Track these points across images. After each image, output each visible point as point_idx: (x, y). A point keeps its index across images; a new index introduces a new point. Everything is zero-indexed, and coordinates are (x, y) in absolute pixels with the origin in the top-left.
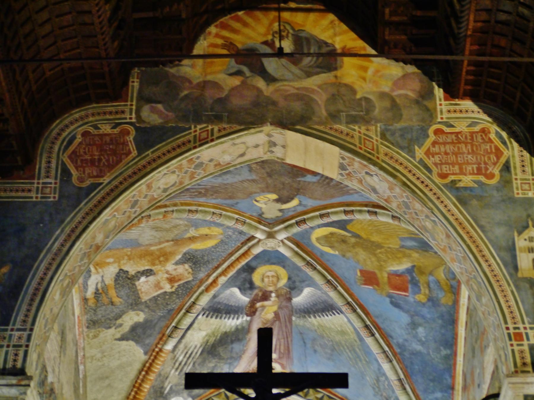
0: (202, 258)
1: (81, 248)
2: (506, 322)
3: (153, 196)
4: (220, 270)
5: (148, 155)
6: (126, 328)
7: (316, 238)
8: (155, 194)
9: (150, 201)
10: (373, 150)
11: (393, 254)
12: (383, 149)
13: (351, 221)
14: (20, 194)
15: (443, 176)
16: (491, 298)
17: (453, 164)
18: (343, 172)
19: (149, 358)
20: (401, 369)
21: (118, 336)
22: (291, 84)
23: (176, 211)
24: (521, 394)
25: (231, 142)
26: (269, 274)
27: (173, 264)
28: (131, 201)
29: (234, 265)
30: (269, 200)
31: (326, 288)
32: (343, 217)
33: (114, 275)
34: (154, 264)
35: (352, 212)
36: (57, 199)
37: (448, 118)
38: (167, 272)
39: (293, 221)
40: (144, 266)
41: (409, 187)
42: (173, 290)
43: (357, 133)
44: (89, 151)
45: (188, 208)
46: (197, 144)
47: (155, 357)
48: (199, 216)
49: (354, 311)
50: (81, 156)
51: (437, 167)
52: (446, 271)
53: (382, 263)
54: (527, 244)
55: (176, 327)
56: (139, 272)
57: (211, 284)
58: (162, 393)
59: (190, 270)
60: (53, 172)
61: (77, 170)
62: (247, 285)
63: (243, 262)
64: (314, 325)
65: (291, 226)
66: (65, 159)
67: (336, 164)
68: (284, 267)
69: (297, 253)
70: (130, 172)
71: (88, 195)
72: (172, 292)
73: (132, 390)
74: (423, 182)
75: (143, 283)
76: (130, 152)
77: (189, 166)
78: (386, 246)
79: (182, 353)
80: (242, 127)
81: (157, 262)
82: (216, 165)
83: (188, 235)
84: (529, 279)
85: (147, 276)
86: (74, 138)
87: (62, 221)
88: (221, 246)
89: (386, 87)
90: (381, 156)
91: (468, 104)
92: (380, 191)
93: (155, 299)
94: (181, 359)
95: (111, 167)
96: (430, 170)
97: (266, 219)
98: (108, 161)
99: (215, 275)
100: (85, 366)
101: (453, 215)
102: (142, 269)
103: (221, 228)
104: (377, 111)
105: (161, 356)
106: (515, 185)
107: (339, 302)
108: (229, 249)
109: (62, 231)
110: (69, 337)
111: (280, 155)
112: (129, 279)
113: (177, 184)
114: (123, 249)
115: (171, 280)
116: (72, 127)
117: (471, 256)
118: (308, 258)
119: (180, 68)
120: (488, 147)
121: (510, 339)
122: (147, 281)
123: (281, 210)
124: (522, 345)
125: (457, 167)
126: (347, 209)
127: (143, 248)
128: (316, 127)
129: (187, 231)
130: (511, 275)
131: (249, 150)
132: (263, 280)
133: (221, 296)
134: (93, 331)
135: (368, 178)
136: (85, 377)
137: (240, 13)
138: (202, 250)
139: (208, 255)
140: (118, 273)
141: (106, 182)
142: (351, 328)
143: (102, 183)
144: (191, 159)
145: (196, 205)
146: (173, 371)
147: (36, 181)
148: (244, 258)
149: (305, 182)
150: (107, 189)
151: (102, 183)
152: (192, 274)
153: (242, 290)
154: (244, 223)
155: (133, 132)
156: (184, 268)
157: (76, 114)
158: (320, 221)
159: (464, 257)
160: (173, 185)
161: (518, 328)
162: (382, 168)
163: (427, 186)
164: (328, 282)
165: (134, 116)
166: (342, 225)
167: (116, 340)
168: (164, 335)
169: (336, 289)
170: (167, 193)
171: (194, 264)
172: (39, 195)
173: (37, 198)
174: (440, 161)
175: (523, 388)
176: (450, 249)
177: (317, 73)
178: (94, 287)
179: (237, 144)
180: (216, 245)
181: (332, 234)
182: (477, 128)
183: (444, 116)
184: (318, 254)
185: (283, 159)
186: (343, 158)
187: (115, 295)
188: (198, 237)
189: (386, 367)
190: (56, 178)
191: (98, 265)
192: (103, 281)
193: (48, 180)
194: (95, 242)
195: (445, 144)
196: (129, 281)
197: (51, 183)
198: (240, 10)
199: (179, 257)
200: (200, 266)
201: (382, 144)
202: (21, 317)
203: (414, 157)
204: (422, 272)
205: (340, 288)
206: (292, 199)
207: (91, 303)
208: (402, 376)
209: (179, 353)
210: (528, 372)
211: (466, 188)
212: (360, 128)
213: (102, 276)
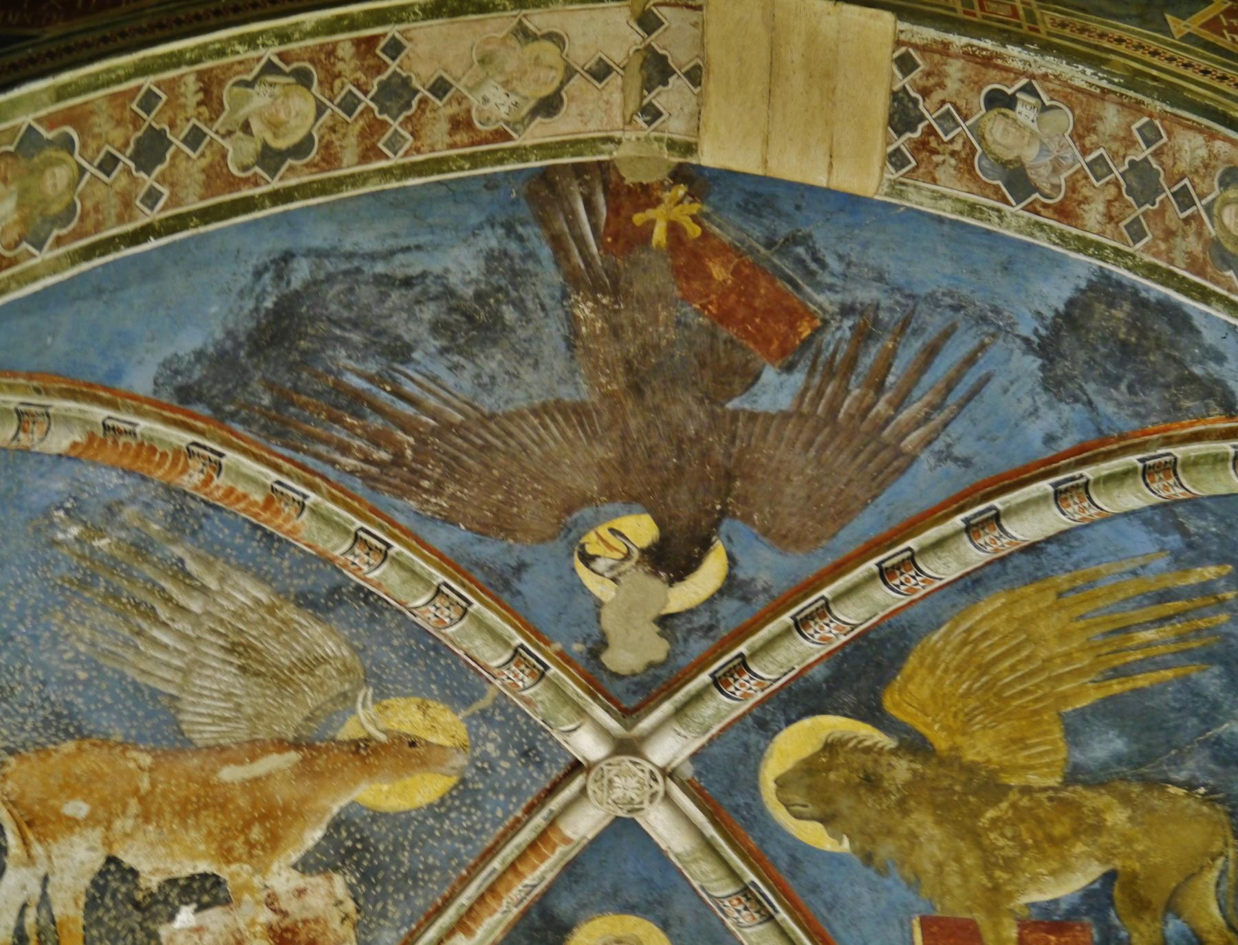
0: (393, 854)
7: (776, 781)
11: (1040, 822)
18: (902, 142)
27: (295, 867)
29: (501, 889)
30: (627, 556)
33: (86, 882)
34: (226, 856)
35: (911, 560)
38: (271, 901)
39: (704, 678)
40: (194, 857)
52: (1223, 888)
53: (1000, 875)
56: (173, 882)
59: (350, 906)
65: (698, 697)
67: (880, 107)
69: (709, 846)
77: (363, 78)
78: (1014, 781)
81: (239, 846)
83: (348, 731)
85: (202, 907)
88: (458, 809)
102: (185, 868)
103: (464, 713)
108: (483, 830)
111: (676, 127)
112: (137, 905)
113: (313, 155)
114: (124, 746)
118: (750, 876)
122: (199, 930)
123: (665, 622)
126: (891, 556)
131: (576, 80)
139: (413, 845)
140: (102, 874)
144: (372, 41)
148: (533, 858)
149: (753, 417)
152: (356, 925)
156: (331, 894)
171: (365, 878)
179: (535, 38)
180: (442, 801)
181: (831, 747)
184: (783, 861)
185: (690, 148)
186: (905, 64)
188: (382, 745)
192: (44, 900)
196: (137, 916)
199: (314, 835)
200: (384, 895)
204: (1141, 906)
213: (46, 879)
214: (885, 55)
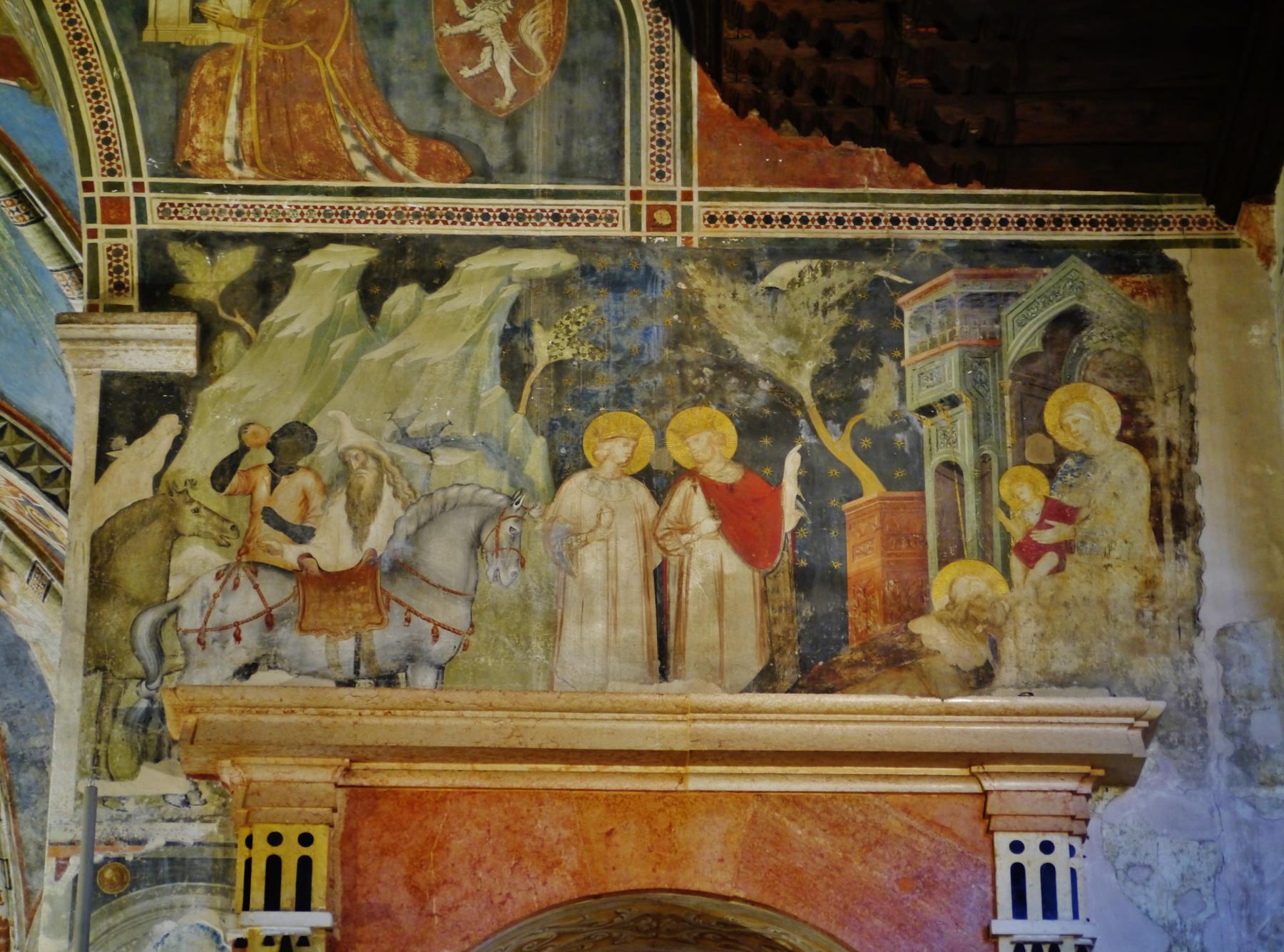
24: (98, 370)
84: (173, 46)
121: (91, 218)
124: (123, 234)
130: (122, 36)
161: (120, 187)
210: (128, 309)
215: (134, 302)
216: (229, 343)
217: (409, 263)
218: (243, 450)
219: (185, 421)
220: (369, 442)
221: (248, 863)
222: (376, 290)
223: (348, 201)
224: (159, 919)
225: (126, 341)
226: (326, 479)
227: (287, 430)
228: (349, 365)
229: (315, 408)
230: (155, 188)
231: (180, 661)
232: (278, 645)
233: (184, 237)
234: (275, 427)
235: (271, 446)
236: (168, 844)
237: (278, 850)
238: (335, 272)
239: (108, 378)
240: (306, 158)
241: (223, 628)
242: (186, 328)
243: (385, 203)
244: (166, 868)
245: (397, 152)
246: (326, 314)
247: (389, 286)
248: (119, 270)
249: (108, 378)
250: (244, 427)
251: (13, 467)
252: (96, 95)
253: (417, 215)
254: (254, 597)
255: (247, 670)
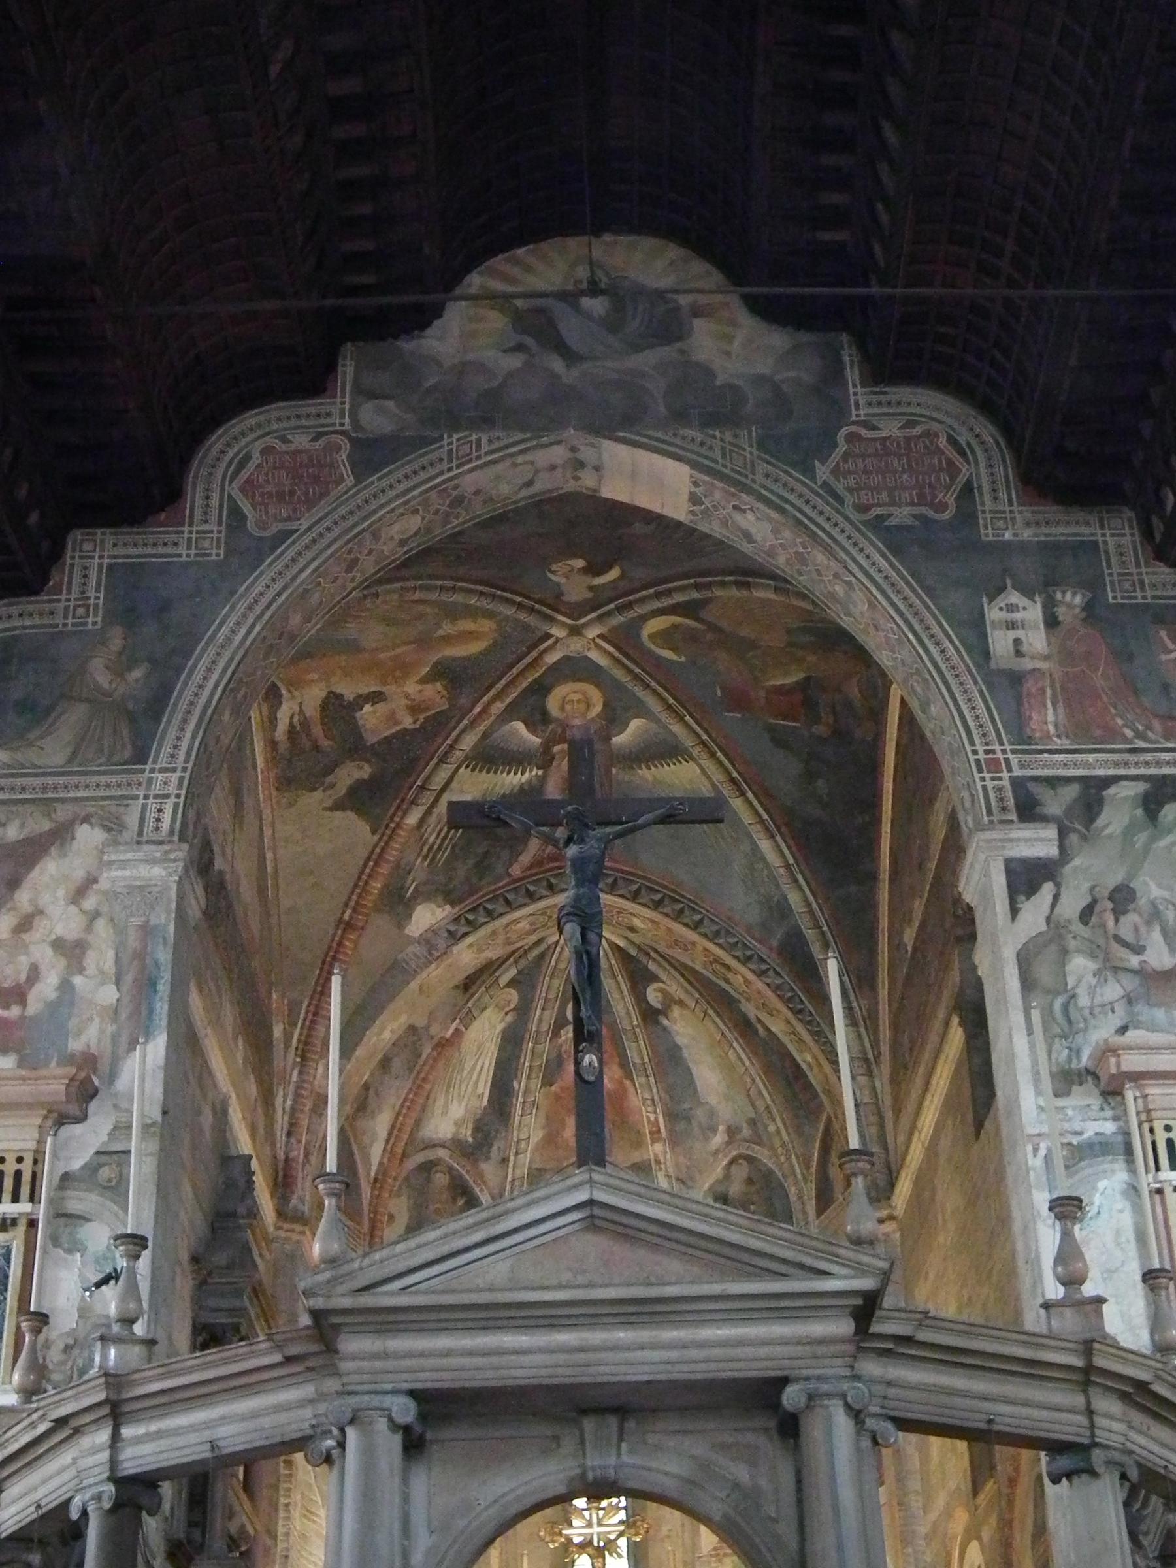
1: (265, 638)
2: (972, 743)
3: (383, 551)
4: (493, 692)
5: (373, 483)
6: (342, 789)
8: (385, 548)
9: (377, 562)
10: (745, 468)
12: (762, 468)
13: (704, 602)
14: (160, 550)
15: (863, 509)
16: (946, 703)
17: (877, 489)
19: (380, 839)
20: (789, 848)
21: (329, 803)
22: (609, 364)
23: (421, 587)
25: (508, 462)
26: (575, 697)
27: (417, 682)
28: (345, 559)
31: (665, 717)
32: (696, 595)
33: (319, 702)
34: (385, 684)
36: (222, 557)
37: (866, 415)
38: (407, 696)
39: (612, 606)
41: (806, 527)
42: (417, 726)
43: (718, 442)
44: (274, 478)
45: (440, 583)
46: (454, 464)
47: (390, 837)
48: (458, 598)
49: (713, 755)
50: (261, 486)
51: (852, 494)
54: (1004, 615)
55: (422, 788)
56: (360, 696)
57: (480, 713)
58: (401, 897)
59: (445, 693)
60: (215, 512)
61: (255, 509)
62: (538, 717)
63: (531, 677)
64: (647, 780)
65: (608, 614)
66: (234, 490)
67: (686, 496)
68: (598, 685)
69: (618, 661)
70: (343, 511)
71: (273, 549)
72: (415, 729)
73: (353, 893)
74: (829, 519)
75: (369, 715)
76: (342, 480)
79: (433, 830)
80: (528, 435)
82: (485, 502)
83: (441, 632)
86: (248, 457)
87: (233, 593)
89: (764, 367)
90: (759, 478)
91: (903, 393)
92: (758, 537)
93: (387, 740)
94: (431, 839)
95: (310, 503)
96: (840, 499)
97: (569, 603)
98: (306, 494)
99: (485, 699)
100: (275, 855)
101: (880, 571)
102: (364, 690)
104: (749, 407)
105: (400, 836)
106: (981, 522)
107: (688, 742)
109: (232, 608)
110: (248, 801)
115: (414, 709)
116: (243, 442)
117: (911, 636)
119: (423, 341)
120: (936, 461)
121: (980, 770)
122: (375, 712)
123: (591, 588)
124: (1000, 779)
125: (884, 494)
126: (700, 580)
127: (367, 655)
128: (651, 433)
129: (438, 625)
130: (978, 667)
131: (541, 475)
132: (562, 708)
133: (495, 735)
134: (286, 794)
135: (738, 517)
136: (276, 871)
137: (520, 252)
138: (464, 658)
140: (327, 698)
141: (303, 528)
142: (706, 782)
143: (297, 530)
145: (452, 578)
146: (419, 860)
147: (186, 528)
150: (306, 540)
151: (297, 530)
153: (531, 726)
154: (532, 610)
155: (346, 445)
157: (250, 419)
158: (657, 605)
159: (899, 641)
160: (416, 534)
161: (993, 752)
162: (761, 498)
163: (836, 525)
164: (669, 707)
165: (347, 420)
166: (689, 609)
167: (325, 809)
168: (403, 800)
169: (682, 719)
170: (405, 549)
172: (193, 552)
173: (188, 556)
174: (857, 483)
175: (1004, 848)
176: (877, 628)
177: (651, 346)
178: (287, 720)
181: (675, 627)
182: (916, 431)
183: (862, 412)
185: (595, 491)
186: (696, 484)
187: (322, 735)
189: (765, 845)
190: (220, 524)
191: (294, 684)
192: (301, 710)
193: (206, 527)
194: (289, 628)
195: (864, 456)
197: (212, 532)
198: (519, 246)
201: (759, 457)
202: (167, 750)
203: (813, 478)
205: (687, 718)
206: (610, 568)
207: (283, 747)
208: (791, 861)
209: (429, 830)
211: (900, 528)
212: (722, 433)
214: (687, 480)
215: (1014, 817)
216: (1073, 838)
217: (1169, 790)
218: (1095, 901)
219: (1058, 885)
220: (1166, 894)
221: (1154, 1144)
222: (1153, 806)
223: (1127, 756)
224: (1099, 1180)
225: (1018, 840)
226: (1145, 915)
227: (1117, 889)
228: (1147, 849)
229: (1131, 876)
230: (1013, 752)
231: (1082, 1025)
232: (1138, 1014)
233: (1035, 779)
234: (1111, 887)
235: (1111, 898)
236: (1096, 1134)
237: (1171, 1135)
238: (1126, 798)
239: (1008, 862)
240: (1098, 733)
241: (1103, 1006)
242: (1051, 832)
243: (1148, 757)
244: (1097, 1148)
245: (1149, 727)
246: (1127, 821)
247: (1161, 805)
248: (1001, 799)
249: (1008, 862)
250: (1092, 888)
251: (711, 940)
252: (969, 700)
253: (1168, 763)
254: (1118, 987)
255: (1123, 1030)
